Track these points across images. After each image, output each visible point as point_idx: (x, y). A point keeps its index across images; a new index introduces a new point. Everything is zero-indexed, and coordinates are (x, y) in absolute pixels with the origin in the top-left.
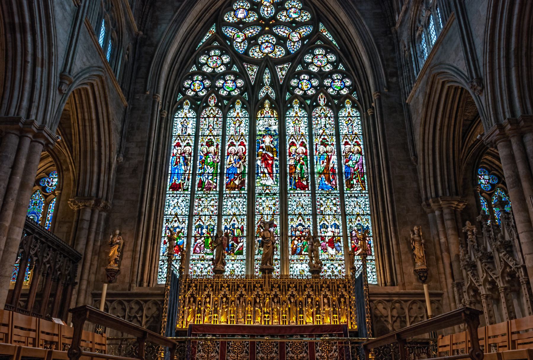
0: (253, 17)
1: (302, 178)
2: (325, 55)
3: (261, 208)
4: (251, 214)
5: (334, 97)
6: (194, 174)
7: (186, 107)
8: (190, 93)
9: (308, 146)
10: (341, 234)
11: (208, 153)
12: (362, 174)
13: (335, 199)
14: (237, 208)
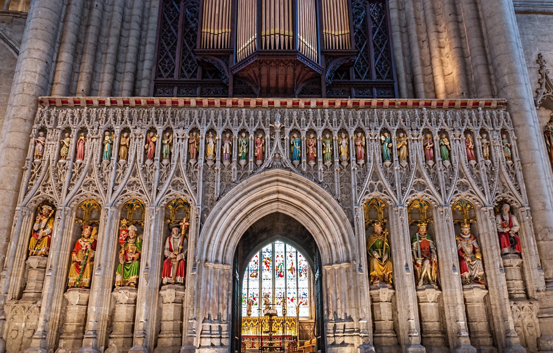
4: (261, 288)
12: (306, 270)
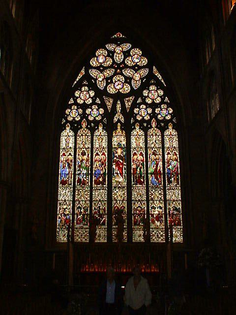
0: (109, 62)
2: (156, 91)
3: (116, 196)
5: (162, 121)
7: (68, 128)
8: (70, 119)
9: (144, 156)
10: (163, 212)
11: (83, 160)
13: (160, 190)
14: (101, 196)
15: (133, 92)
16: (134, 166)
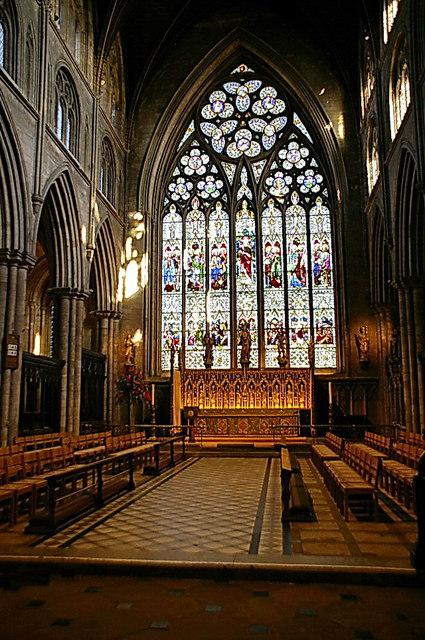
0: (229, 110)
1: (277, 276)
6: (184, 277)
7: (173, 211)
9: (282, 246)
11: (195, 256)
15: (265, 155)
16: (266, 262)
